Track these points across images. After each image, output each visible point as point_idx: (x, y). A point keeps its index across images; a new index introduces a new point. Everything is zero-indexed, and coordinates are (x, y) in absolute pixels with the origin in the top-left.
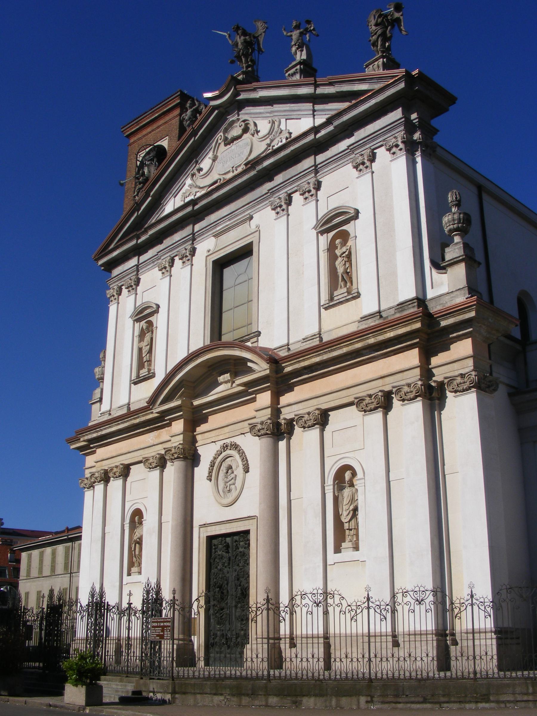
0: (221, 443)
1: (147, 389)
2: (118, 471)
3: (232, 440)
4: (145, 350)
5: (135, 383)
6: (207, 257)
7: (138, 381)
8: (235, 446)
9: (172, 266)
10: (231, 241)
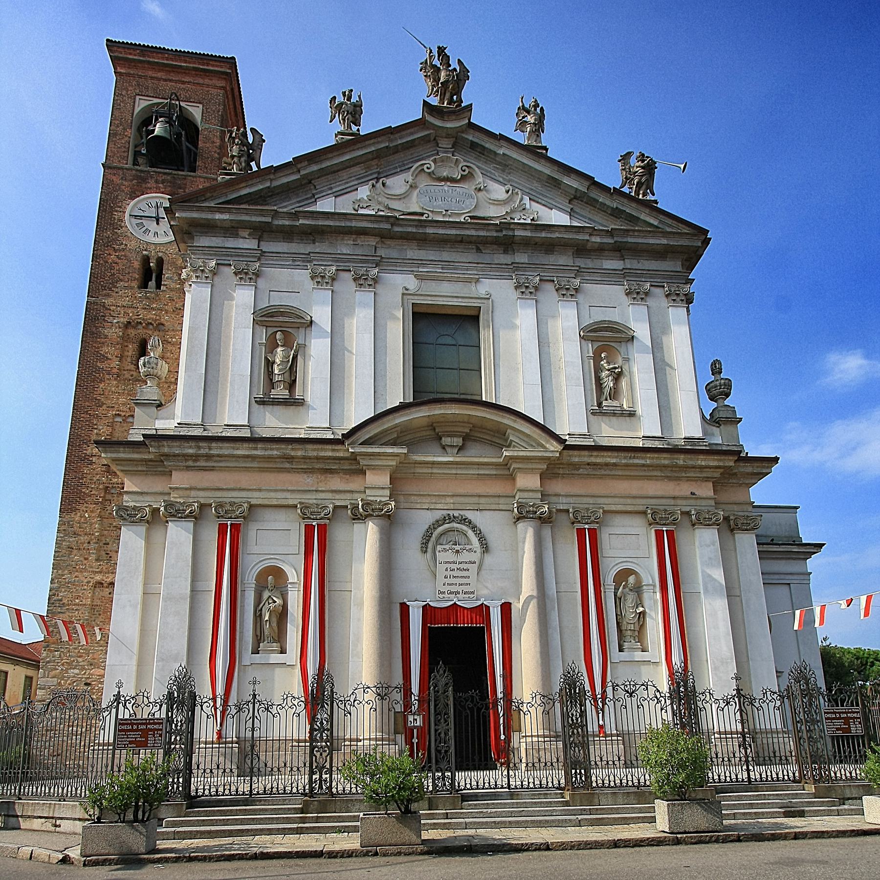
0: (445, 512)
3: (462, 513)
5: (261, 402)
6: (403, 294)
10: (447, 293)
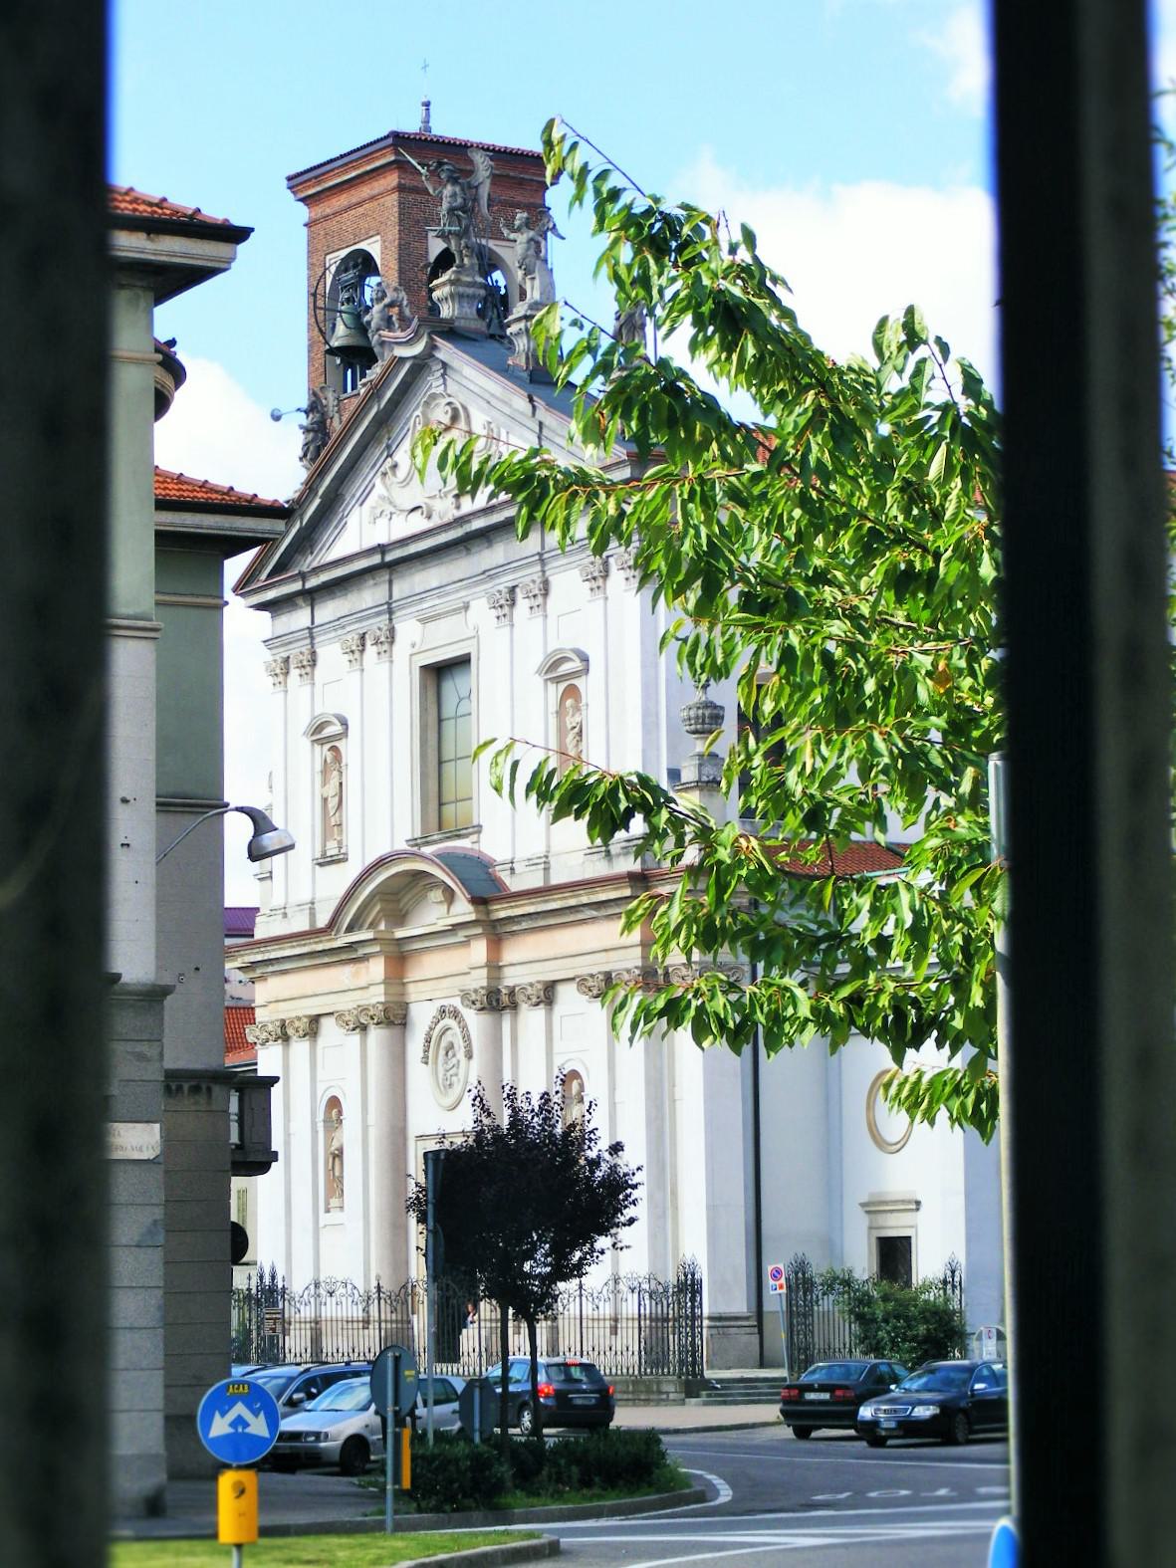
0: (437, 1004)
1: (339, 879)
2: (303, 1025)
4: (333, 803)
7: (326, 861)
8: (456, 1014)
9: (362, 651)
